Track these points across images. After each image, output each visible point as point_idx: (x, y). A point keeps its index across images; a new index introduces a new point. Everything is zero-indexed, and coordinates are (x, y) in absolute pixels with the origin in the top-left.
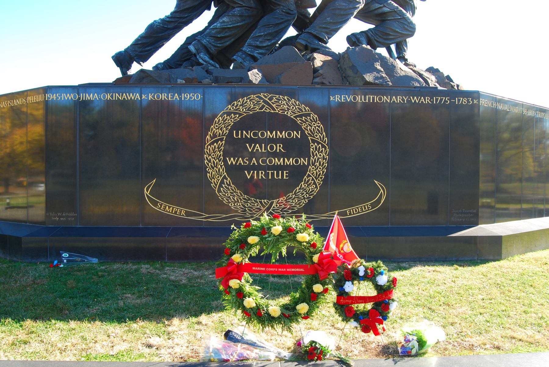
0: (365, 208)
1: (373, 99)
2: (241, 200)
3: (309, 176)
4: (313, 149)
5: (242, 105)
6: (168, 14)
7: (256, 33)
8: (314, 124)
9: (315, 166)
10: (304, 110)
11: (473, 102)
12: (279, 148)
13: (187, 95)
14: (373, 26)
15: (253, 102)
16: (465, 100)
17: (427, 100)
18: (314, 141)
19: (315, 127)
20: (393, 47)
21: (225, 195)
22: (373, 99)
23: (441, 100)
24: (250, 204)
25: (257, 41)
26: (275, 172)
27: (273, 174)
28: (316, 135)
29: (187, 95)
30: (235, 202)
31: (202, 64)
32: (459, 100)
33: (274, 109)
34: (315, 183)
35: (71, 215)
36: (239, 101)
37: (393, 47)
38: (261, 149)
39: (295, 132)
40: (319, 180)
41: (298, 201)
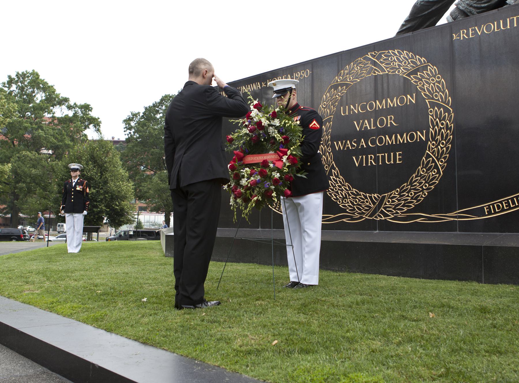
0: (513, 203)
2: (349, 195)
3: (428, 156)
4: (432, 116)
5: (349, 73)
8: (433, 80)
9: (436, 141)
10: (419, 63)
12: (390, 121)
13: (298, 75)
15: (360, 67)
18: (433, 105)
19: (434, 84)
21: (332, 190)
24: (359, 200)
26: (386, 154)
28: (436, 96)
29: (298, 75)
30: (344, 198)
33: (383, 71)
34: (436, 167)
36: (346, 69)
38: (370, 127)
39: (409, 96)
40: (442, 162)
41: (415, 193)
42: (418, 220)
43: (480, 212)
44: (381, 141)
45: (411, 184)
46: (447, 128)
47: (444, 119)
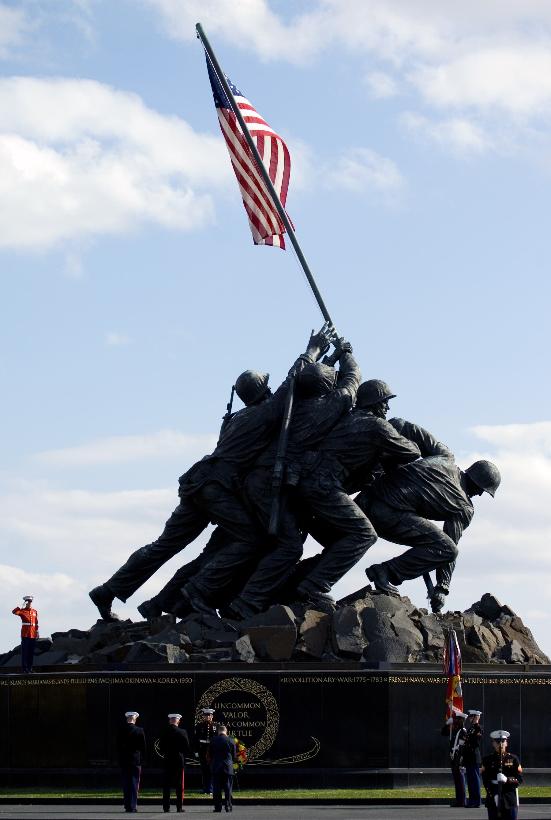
1: (311, 680)
3: (266, 734)
5: (220, 686)
6: (155, 538)
7: (256, 577)
11: (383, 680)
12: (245, 715)
14: (411, 548)
16: (377, 679)
17: (350, 680)
18: (269, 710)
20: (433, 574)
22: (311, 680)
23: (360, 679)
25: (256, 587)
27: (241, 733)
31: (197, 612)
32: (373, 679)
33: (242, 689)
34: (270, 739)
35: (104, 761)
37: (433, 574)
42: (260, 764)
43: (291, 760)
44: (240, 724)
45: (257, 746)
46: (276, 722)
47: (275, 717)
